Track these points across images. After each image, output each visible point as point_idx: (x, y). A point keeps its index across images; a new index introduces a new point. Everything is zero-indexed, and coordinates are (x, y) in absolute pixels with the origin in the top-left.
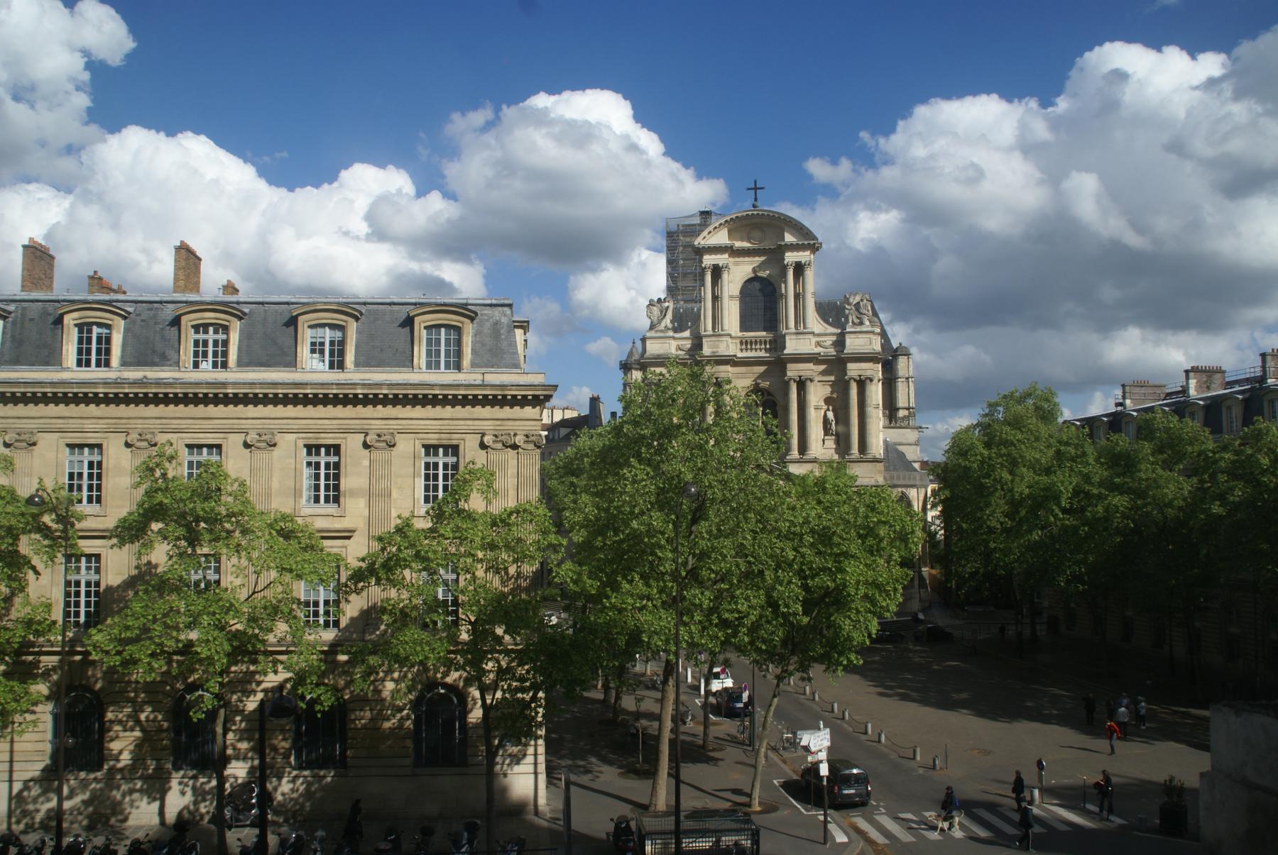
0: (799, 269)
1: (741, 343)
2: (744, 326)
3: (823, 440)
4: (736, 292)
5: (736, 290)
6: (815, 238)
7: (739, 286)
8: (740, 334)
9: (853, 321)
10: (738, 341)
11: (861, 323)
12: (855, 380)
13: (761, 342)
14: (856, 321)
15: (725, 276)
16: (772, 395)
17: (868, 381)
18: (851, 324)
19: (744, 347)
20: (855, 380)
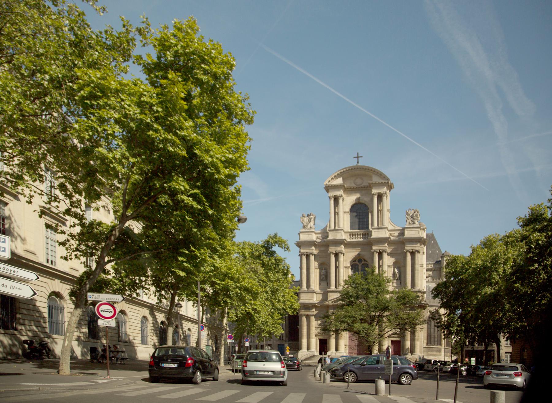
0: (380, 197)
1: (350, 235)
2: (352, 227)
4: (348, 210)
5: (347, 208)
6: (388, 179)
7: (349, 207)
8: (349, 230)
9: (409, 223)
10: (348, 234)
11: (414, 223)
12: (409, 252)
13: (360, 234)
14: (411, 222)
15: (341, 201)
16: (367, 261)
17: (417, 253)
18: (408, 224)
19: (351, 236)
20: (409, 252)
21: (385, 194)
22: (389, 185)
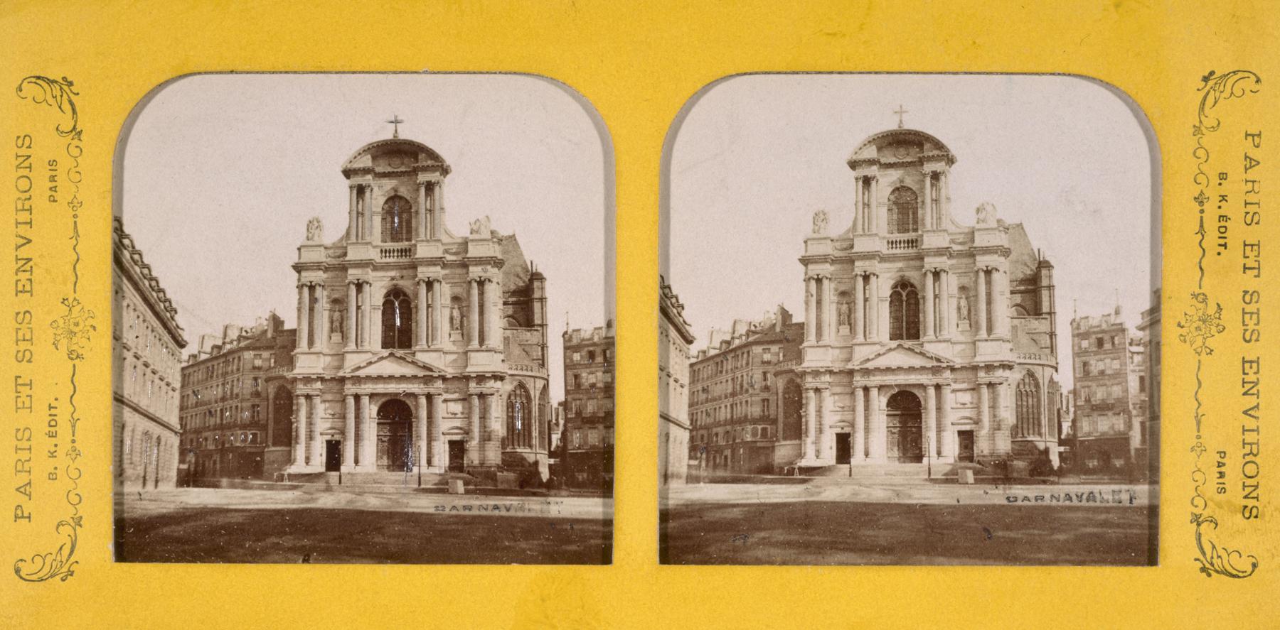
1: (382, 251)
3: (450, 335)
10: (379, 250)
21: (438, 183)
22: (443, 169)
